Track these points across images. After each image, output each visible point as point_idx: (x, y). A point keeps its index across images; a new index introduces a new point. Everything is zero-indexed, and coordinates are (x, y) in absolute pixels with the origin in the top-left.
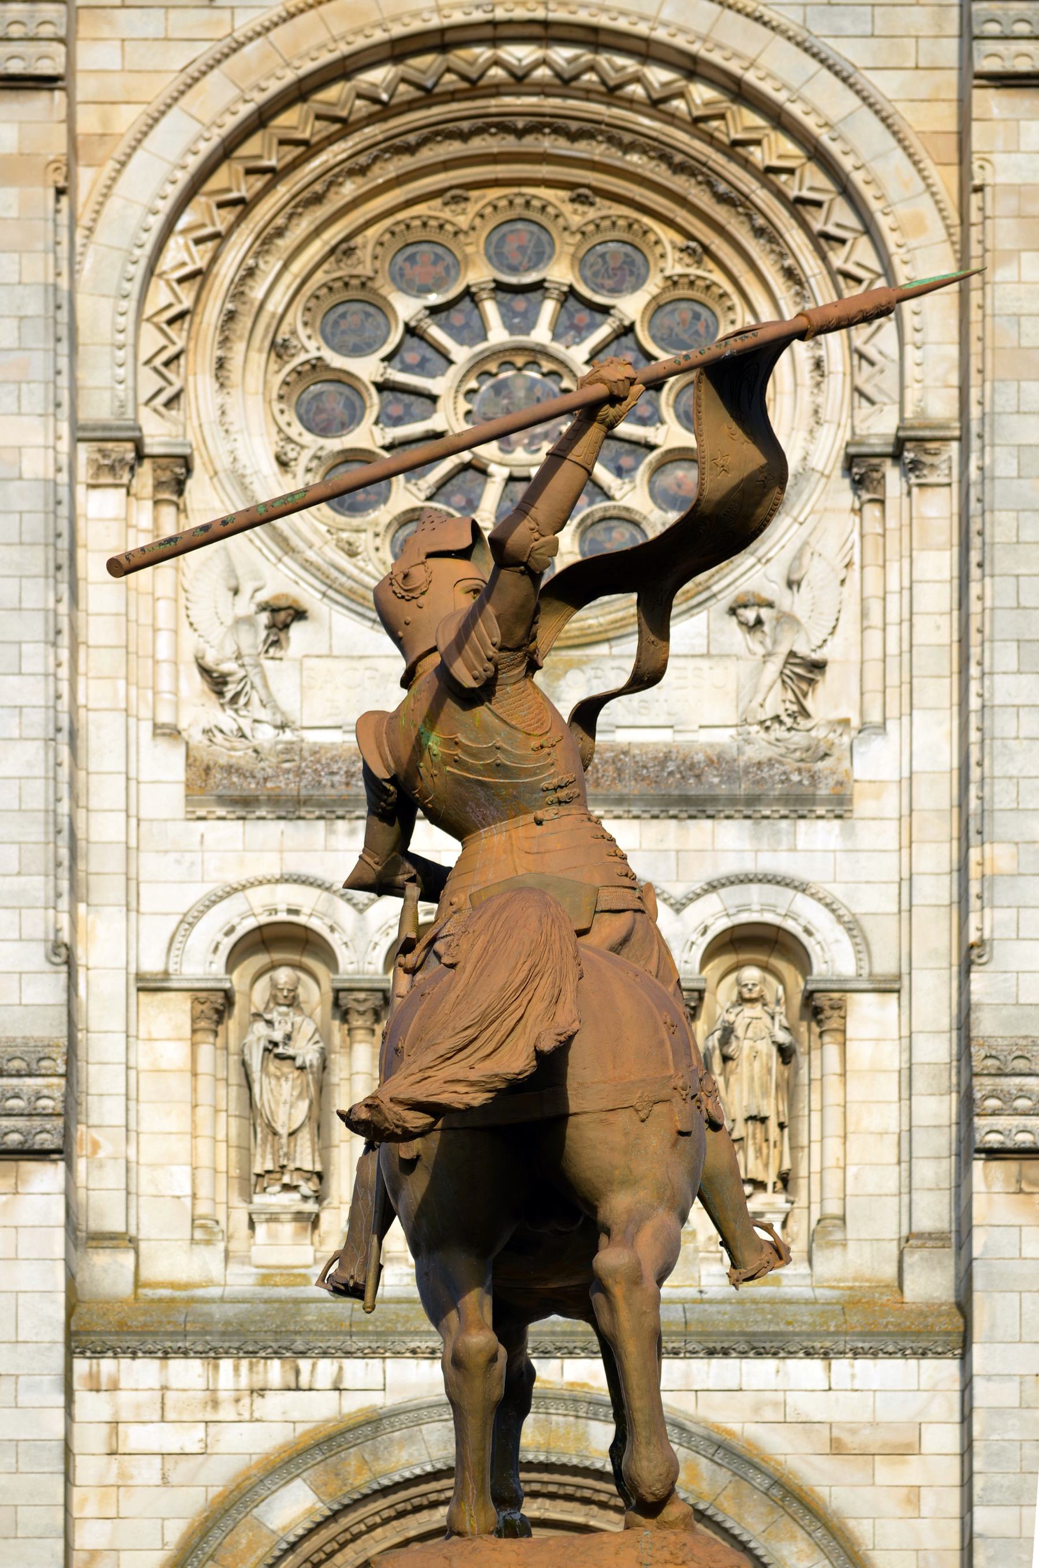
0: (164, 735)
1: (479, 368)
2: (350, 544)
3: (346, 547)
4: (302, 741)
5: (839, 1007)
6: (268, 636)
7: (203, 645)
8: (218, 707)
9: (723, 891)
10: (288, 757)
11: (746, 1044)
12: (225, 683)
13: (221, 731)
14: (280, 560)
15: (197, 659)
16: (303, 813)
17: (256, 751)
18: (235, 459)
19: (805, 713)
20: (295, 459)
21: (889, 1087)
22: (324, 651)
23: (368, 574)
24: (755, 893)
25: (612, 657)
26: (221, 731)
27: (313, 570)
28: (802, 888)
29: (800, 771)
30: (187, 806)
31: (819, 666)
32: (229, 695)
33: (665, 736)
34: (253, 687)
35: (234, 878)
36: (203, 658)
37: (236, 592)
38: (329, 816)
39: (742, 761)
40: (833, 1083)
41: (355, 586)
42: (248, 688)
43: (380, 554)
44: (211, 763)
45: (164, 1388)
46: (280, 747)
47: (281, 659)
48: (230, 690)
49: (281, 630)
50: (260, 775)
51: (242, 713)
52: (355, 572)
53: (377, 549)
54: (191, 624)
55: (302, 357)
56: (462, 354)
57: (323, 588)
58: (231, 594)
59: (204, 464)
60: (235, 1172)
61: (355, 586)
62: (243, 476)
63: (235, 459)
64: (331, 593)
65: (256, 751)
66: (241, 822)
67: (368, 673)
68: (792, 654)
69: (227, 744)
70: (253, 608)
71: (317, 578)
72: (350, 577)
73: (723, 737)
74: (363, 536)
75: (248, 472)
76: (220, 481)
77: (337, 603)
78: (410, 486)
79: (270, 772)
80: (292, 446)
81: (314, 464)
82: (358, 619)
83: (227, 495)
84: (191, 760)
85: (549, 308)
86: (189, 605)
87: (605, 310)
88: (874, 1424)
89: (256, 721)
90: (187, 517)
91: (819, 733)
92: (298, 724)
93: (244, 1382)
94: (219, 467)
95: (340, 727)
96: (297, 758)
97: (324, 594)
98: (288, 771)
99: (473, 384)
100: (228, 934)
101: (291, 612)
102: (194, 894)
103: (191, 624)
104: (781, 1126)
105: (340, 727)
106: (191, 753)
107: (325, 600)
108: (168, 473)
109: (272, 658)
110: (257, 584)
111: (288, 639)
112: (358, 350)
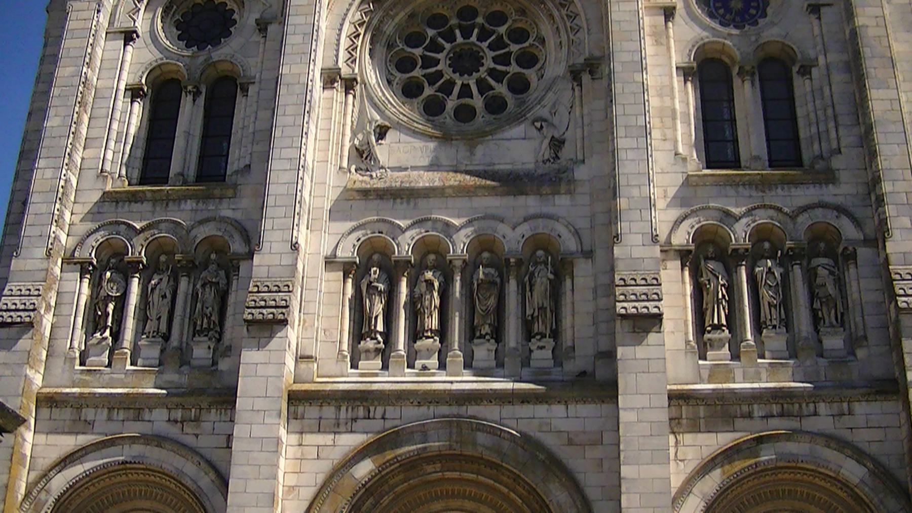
5: (572, 264)
9: (530, 222)
11: (539, 280)
19: (557, 157)
21: (590, 296)
25: (493, 140)
29: (555, 177)
31: (563, 142)
33: (509, 167)
39: (536, 174)
40: (569, 293)
45: (320, 418)
48: (365, 156)
55: (397, 49)
56: (448, 46)
60: (356, 332)
68: (553, 137)
73: (531, 166)
87: (494, 32)
88: (584, 432)
91: (564, 163)
93: (349, 415)
99: (452, 55)
100: (358, 241)
104: (551, 311)
112: (416, 47)
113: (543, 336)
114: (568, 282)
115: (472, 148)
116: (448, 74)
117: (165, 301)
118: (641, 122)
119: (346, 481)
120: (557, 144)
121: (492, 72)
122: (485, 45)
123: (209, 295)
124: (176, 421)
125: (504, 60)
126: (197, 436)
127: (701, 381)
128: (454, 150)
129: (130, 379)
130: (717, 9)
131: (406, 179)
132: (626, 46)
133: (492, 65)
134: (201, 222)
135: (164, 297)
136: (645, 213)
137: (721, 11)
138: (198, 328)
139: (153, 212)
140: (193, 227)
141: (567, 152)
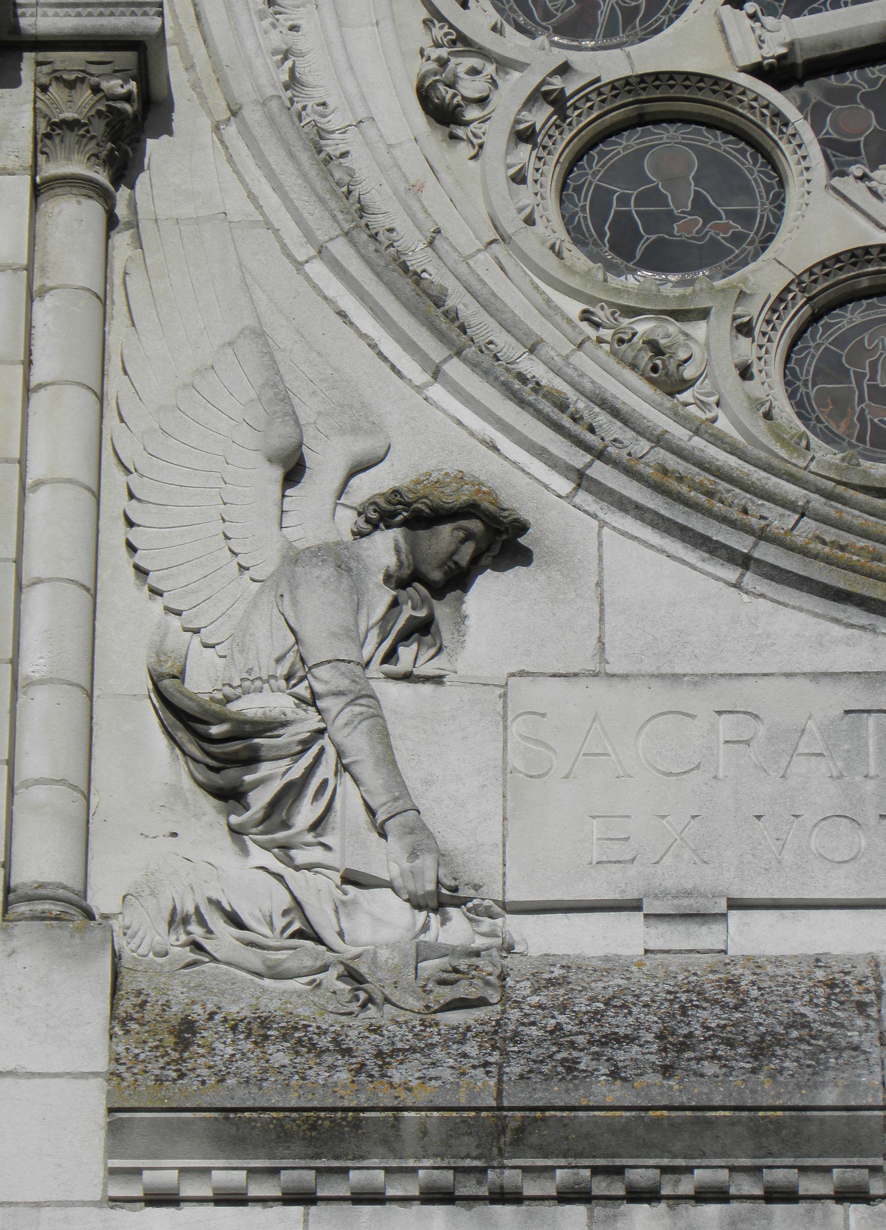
0: (42, 917)
2: (656, 348)
3: (645, 359)
4: (508, 948)
6: (395, 603)
7: (177, 639)
8: (226, 839)
10: (463, 990)
12: (252, 759)
13: (235, 920)
14: (436, 373)
15: (156, 680)
16: (511, 1178)
17: (352, 976)
18: (293, 81)
20: (482, 101)
22: (584, 661)
23: (719, 440)
26: (235, 920)
27: (547, 407)
30: (111, 1152)
32: (259, 800)
34: (343, 767)
36: (180, 676)
38: (600, 1186)
41: (673, 462)
42: (326, 770)
43: (754, 387)
44: (198, 1013)
46: (430, 966)
47: (437, 680)
49: (438, 591)
50: (365, 1050)
51: (300, 856)
52: (679, 433)
53: (745, 372)
54: (141, 572)
57: (579, 459)
58: (277, 473)
59: (196, 86)
61: (673, 462)
62: (322, 133)
63: (293, 81)
64: (600, 472)
65: (352, 976)
66: (297, 1211)
67: (725, 726)
69: (253, 958)
70: (347, 519)
71: (557, 427)
72: (659, 440)
74: (699, 330)
75: (334, 121)
76: (246, 132)
77: (623, 504)
78: (847, 185)
79: (403, 1037)
80: (475, 62)
81: (541, 115)
82: (692, 556)
83: (271, 176)
84: (126, 1005)
86: (135, 536)
89: (351, 879)
90: (138, 242)
92: (493, 892)
94: (244, 91)
95: (635, 906)
96: (494, 997)
97: (581, 479)
98: (463, 1035)
101: (475, 525)
103: (141, 572)
105: (635, 906)
106: (128, 983)
107: (583, 498)
108: (85, 96)
109: (407, 677)
110: (362, 446)
111: (461, 619)
131: (711, 1017)
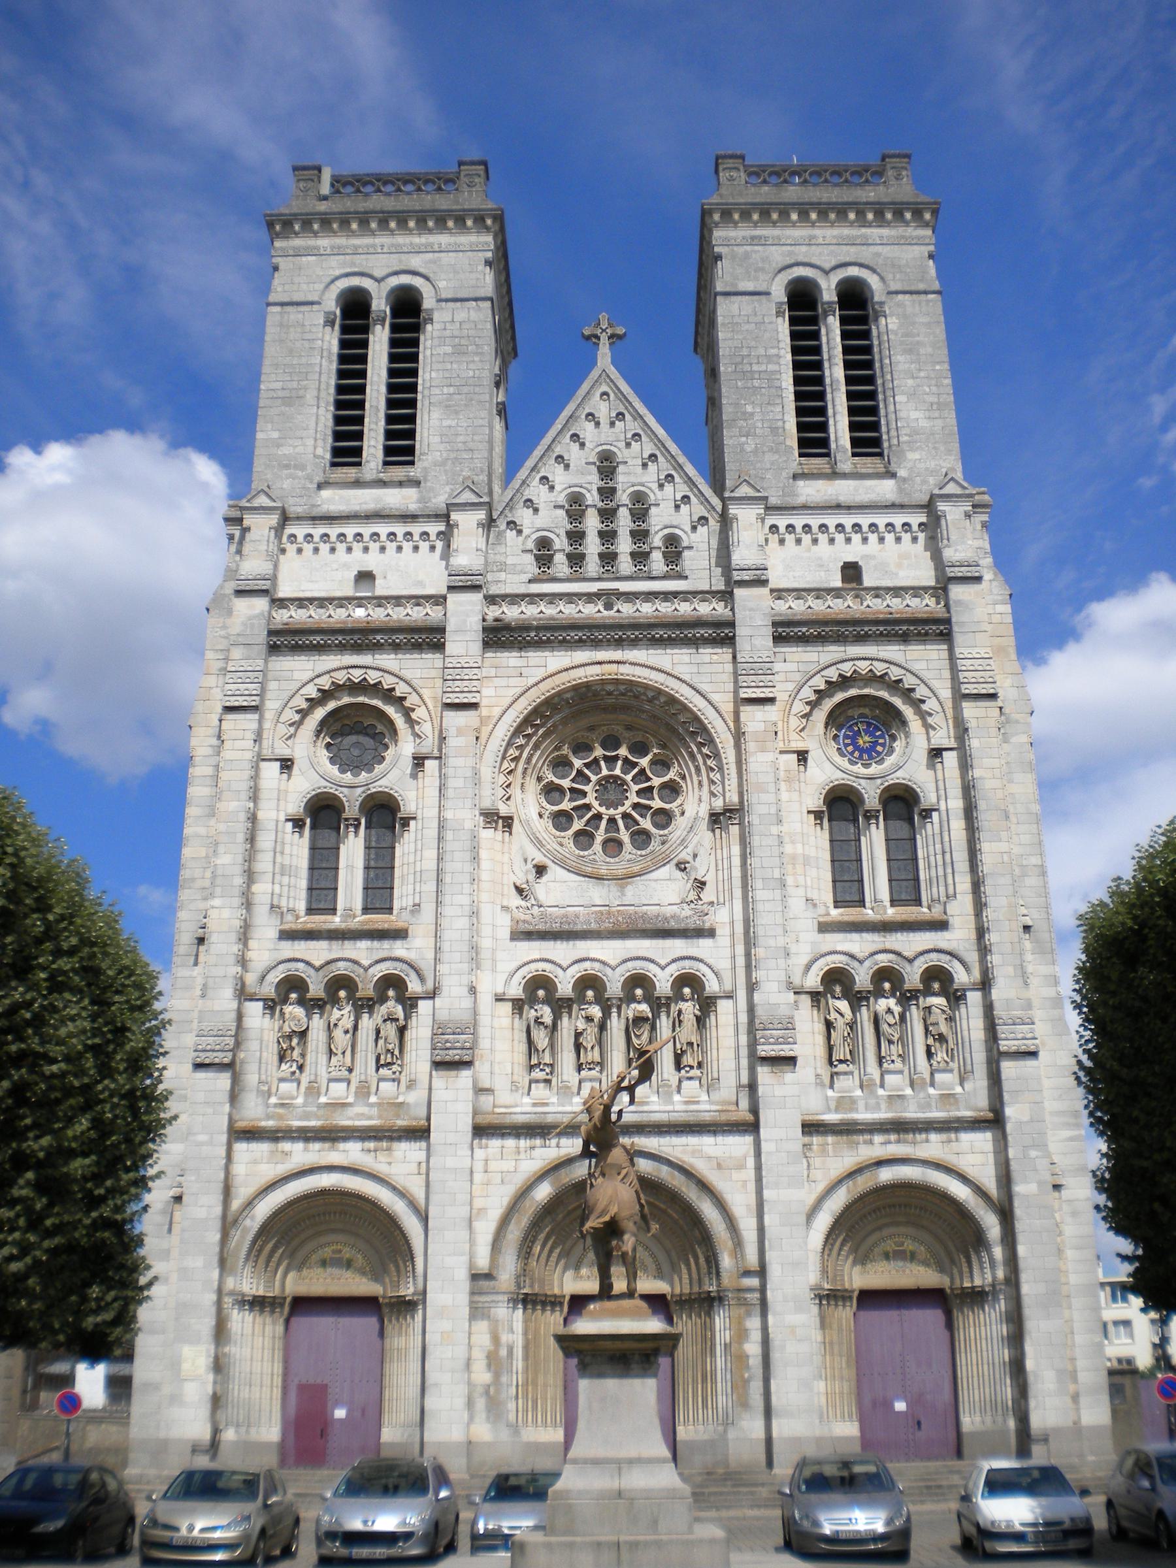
1: (599, 783)
24: (687, 963)
28: (701, 961)
31: (704, 883)
35: (526, 959)
37: (526, 861)
56: (594, 778)
85: (620, 763)
102: (515, 965)
113: (692, 1067)
114: (713, 1017)
115: (622, 888)
116: (597, 807)
117: (348, 1035)
118: (777, 874)
119: (527, 1203)
120: (701, 884)
121: (636, 806)
122: (635, 788)
123: (390, 1030)
124: (369, 1151)
125: (647, 792)
126: (390, 1163)
127: (829, 1111)
128: (606, 889)
129: (321, 1112)
130: (846, 745)
132: (764, 797)
133: (637, 800)
134: (378, 962)
135: (347, 1032)
136: (781, 962)
137: (850, 748)
138: (382, 1062)
139: (330, 950)
140: (371, 966)
141: (708, 895)
